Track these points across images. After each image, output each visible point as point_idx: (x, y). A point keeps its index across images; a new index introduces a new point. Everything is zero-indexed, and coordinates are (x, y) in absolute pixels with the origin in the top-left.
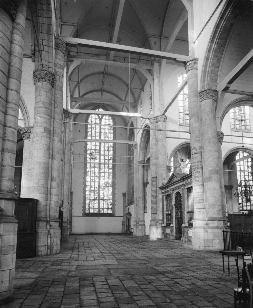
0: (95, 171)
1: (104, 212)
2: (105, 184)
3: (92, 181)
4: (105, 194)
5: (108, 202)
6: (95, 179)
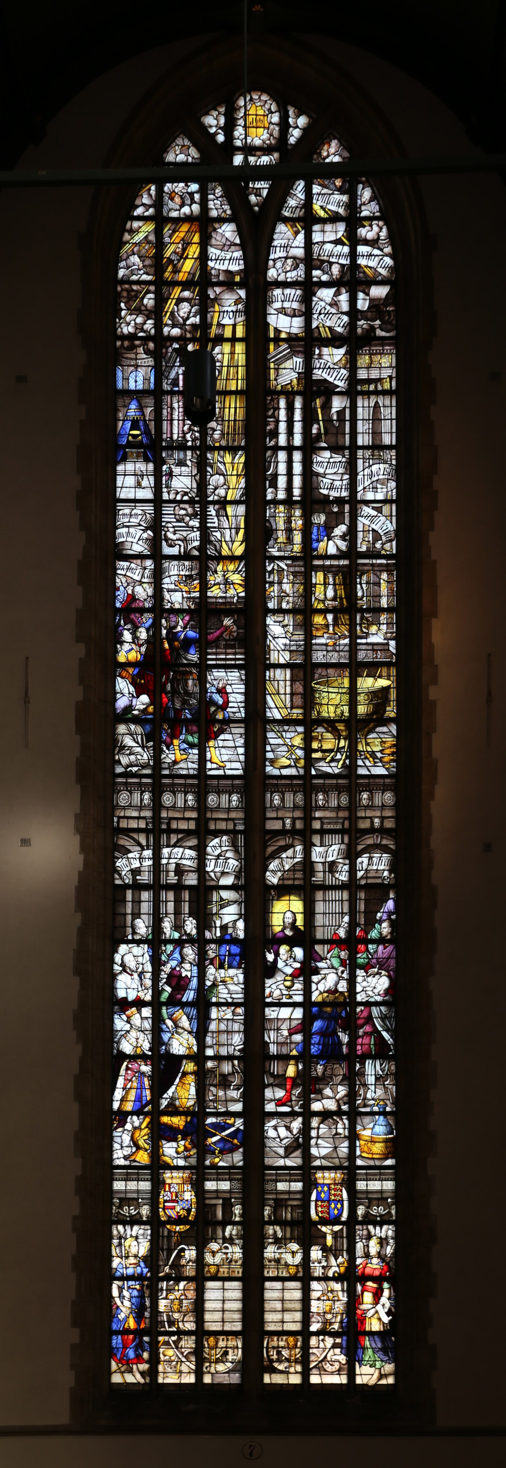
0: (201, 869)
1: (305, 1374)
2: (317, 1025)
3: (174, 1001)
4: (321, 1149)
5: (351, 1251)
6: (211, 970)
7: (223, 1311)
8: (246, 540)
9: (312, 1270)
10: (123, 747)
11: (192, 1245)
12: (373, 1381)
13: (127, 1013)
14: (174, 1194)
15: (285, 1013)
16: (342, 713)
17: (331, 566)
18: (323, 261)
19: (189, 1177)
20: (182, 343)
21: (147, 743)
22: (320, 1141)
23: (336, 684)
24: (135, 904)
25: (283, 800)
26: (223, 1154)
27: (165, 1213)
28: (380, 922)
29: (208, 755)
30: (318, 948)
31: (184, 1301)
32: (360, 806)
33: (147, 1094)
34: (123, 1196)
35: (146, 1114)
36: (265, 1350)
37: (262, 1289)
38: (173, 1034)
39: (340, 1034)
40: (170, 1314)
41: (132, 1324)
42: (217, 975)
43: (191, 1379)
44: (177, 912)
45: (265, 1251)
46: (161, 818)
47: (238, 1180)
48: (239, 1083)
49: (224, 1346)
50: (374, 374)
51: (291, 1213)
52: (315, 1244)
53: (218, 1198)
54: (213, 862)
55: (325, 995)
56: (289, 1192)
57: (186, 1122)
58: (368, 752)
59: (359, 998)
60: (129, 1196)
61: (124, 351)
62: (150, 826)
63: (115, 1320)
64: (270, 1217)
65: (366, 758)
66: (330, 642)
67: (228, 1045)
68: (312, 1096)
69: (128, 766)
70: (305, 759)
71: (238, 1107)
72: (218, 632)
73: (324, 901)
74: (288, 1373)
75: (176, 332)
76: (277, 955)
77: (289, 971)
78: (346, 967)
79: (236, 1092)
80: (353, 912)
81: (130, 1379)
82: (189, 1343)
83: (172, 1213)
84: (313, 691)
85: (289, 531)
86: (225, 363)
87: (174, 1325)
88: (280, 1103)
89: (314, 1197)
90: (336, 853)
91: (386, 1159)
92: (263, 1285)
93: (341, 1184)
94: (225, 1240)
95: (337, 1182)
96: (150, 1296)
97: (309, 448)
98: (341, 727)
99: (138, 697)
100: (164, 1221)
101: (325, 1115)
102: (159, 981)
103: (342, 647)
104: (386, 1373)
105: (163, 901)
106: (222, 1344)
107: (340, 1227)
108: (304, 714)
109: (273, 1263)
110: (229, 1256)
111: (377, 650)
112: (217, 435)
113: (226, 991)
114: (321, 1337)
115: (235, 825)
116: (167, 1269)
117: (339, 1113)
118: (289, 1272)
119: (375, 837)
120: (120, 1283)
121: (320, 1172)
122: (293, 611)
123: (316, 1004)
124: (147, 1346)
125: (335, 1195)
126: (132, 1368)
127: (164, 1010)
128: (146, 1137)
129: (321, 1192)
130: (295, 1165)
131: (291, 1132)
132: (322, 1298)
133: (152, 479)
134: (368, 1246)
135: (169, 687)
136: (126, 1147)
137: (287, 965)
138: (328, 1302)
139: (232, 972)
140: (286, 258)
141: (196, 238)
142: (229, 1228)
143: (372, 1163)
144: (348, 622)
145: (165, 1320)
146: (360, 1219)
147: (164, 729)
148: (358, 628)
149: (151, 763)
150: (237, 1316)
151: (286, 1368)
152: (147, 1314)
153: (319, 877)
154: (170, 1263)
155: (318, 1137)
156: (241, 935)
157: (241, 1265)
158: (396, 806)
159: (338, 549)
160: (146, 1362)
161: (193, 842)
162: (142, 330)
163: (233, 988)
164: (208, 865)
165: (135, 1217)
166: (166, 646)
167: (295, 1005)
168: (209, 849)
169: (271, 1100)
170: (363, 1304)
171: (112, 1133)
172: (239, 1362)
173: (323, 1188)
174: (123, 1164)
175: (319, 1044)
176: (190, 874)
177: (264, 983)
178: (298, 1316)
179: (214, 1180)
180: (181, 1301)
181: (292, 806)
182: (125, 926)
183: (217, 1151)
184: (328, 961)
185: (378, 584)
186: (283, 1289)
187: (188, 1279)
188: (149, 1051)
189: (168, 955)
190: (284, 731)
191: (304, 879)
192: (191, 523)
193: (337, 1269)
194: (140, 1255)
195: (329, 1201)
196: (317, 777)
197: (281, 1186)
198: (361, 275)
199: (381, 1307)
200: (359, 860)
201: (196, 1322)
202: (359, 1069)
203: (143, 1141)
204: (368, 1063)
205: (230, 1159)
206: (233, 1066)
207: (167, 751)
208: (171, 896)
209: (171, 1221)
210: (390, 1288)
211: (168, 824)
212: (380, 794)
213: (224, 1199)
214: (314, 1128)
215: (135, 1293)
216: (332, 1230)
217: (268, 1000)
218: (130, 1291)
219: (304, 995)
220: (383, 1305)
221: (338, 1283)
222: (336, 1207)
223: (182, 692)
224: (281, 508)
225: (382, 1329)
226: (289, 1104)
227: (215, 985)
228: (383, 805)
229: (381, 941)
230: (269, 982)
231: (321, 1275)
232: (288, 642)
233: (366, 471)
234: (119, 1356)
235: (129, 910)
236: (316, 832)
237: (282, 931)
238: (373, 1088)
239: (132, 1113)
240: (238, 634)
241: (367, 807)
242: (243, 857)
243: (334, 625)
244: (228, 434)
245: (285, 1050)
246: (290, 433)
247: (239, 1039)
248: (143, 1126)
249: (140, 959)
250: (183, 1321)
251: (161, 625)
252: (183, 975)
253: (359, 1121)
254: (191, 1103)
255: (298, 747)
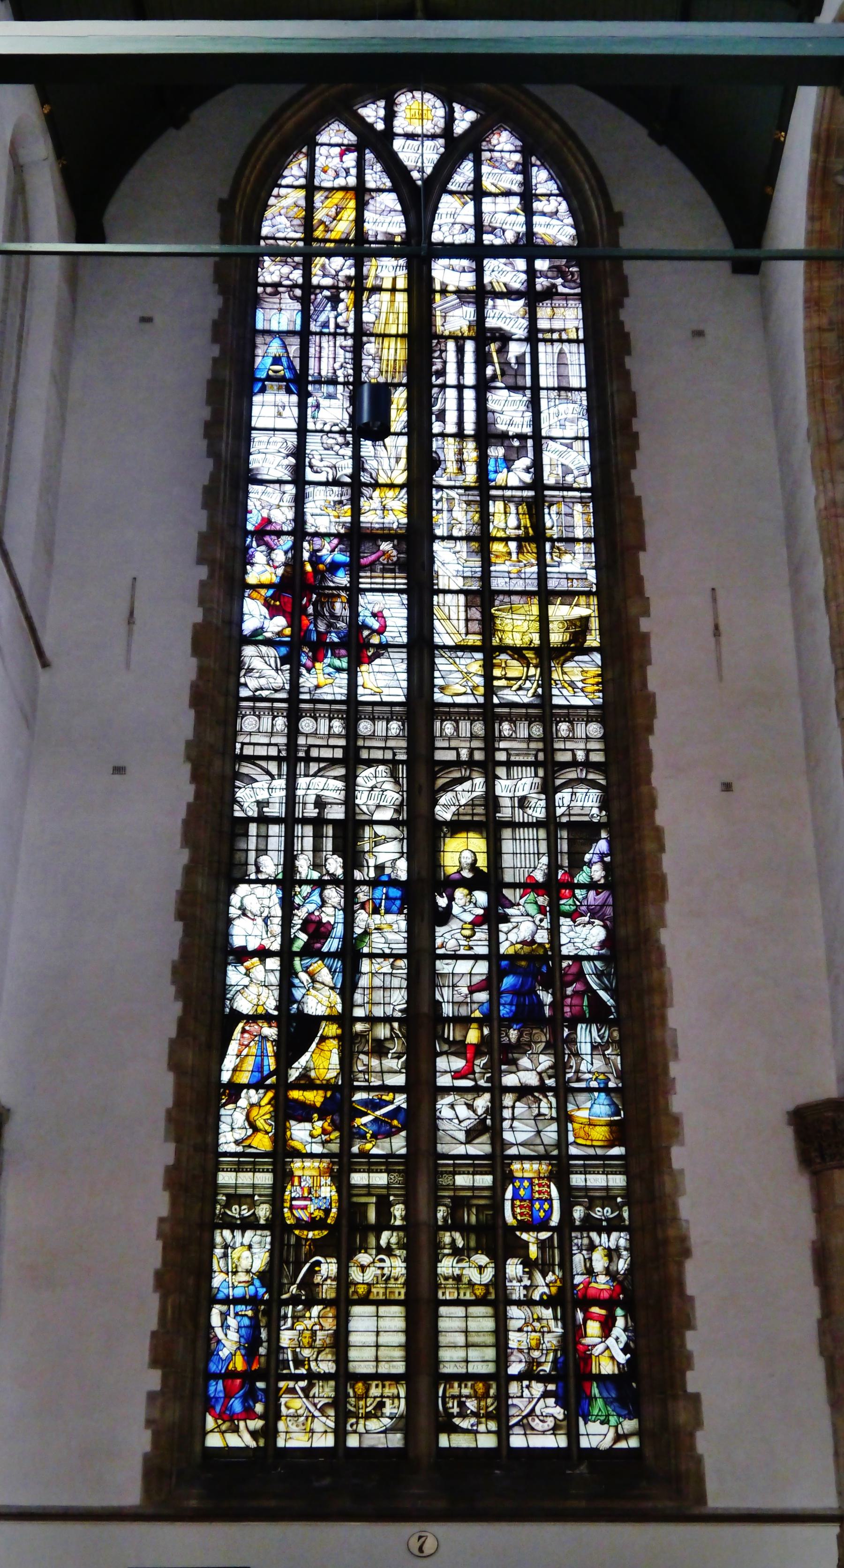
0: (349, 801)
1: (503, 1433)
2: (508, 981)
3: (309, 951)
7: (377, 1346)
8: (409, 468)
9: (508, 1291)
10: (250, 670)
11: (332, 1256)
12: (606, 1444)
13: (245, 964)
14: (306, 1190)
15: (463, 966)
16: (531, 642)
17: (512, 497)
18: (495, 228)
19: (328, 1168)
20: (334, 290)
21: (282, 665)
22: (516, 1124)
23: (522, 611)
24: (260, 839)
25: (457, 729)
26: (377, 1139)
27: (292, 1214)
28: (590, 864)
29: (360, 681)
30: (508, 893)
31: (318, 1333)
32: (557, 737)
33: (271, 1063)
34: (232, 1191)
35: (268, 1088)
36: (440, 1400)
37: (436, 1317)
38: (308, 990)
39: (540, 993)
40: (298, 1350)
41: (239, 1364)
42: (370, 921)
43: (329, 1441)
44: (317, 849)
45: (439, 1265)
46: (297, 745)
47: (399, 1171)
48: (400, 1050)
49: (379, 1395)
50: (557, 325)
51: (477, 1216)
52: (513, 1257)
53: (369, 1195)
54: (366, 794)
55: (519, 946)
56: (473, 1188)
57: (325, 1097)
58: (565, 681)
59: (565, 951)
60: (241, 1191)
61: (265, 296)
62: (284, 754)
63: (215, 1358)
64: (445, 1219)
65: (563, 687)
66: (514, 570)
67: (384, 1004)
68: (503, 1067)
69: (257, 690)
70: (485, 686)
71: (400, 1080)
72: (373, 557)
73: (514, 839)
74: (476, 1432)
75: (328, 282)
76: (451, 899)
77: (469, 918)
78: (545, 915)
79: (396, 1061)
80: (552, 852)
81: (234, 1441)
82: (325, 1391)
83: (304, 1215)
84: (493, 618)
85: (461, 462)
86: (384, 309)
87: (303, 1366)
88: (458, 1075)
89: (509, 1194)
90: (527, 787)
91: (611, 1146)
92: (437, 1311)
93: (549, 1179)
94: (379, 1250)
95: (542, 1175)
96: (268, 1326)
97: (483, 387)
98: (530, 655)
99: (271, 619)
100: (291, 1225)
101: (522, 1092)
102: (290, 927)
103: (527, 576)
104: (626, 1432)
105: (298, 837)
106: (374, 1391)
107: (549, 1234)
108: (483, 640)
109: (450, 1281)
110: (386, 1271)
111: (572, 579)
112: (372, 373)
113: (383, 940)
114: (526, 1383)
115: (394, 754)
116: (294, 1289)
117: (542, 1088)
118: (475, 1294)
119: (579, 771)
120: (224, 1308)
121: (518, 1162)
122: (468, 538)
123: (506, 957)
124: (261, 1395)
125: (540, 1192)
126: (238, 1426)
127: (297, 962)
128: (268, 1116)
129: (519, 1188)
130: (482, 1153)
131: (474, 1111)
132: (525, 1329)
133: (295, 411)
134: (590, 1259)
135: (310, 610)
136: (239, 1128)
137: (465, 911)
138: (533, 1334)
139: (390, 918)
140: (453, 224)
141: (352, 204)
142: (385, 1235)
143: (591, 1151)
144: (535, 550)
145: (290, 1358)
146: (577, 1223)
147: (304, 652)
148: (548, 557)
149: (287, 687)
150: (399, 1353)
151: (472, 1425)
152: (262, 1351)
153: (505, 813)
154: (298, 1281)
155: (513, 1119)
156: (403, 876)
157: (404, 1284)
158: (604, 738)
159: (521, 480)
160: (260, 1417)
161: (341, 771)
162: (288, 278)
163: (391, 936)
164: (359, 797)
165: (248, 1220)
166: (308, 568)
167: (477, 958)
168: (359, 780)
169: (446, 1072)
170: (586, 1336)
171: (219, 1111)
172: (401, 1417)
173: (522, 1183)
174: (233, 1150)
175: (511, 1004)
176: (335, 806)
177: (434, 932)
178: (491, 1353)
179: (364, 1171)
180: (314, 1333)
181: (469, 735)
182: (246, 864)
183: (368, 1135)
184: (521, 907)
185: (571, 515)
186: (466, 1317)
187: (326, 1303)
188: (275, 1009)
189: (304, 898)
190: (458, 657)
191: (486, 815)
192: (342, 452)
193: (546, 1290)
194: (254, 1270)
195: (532, 1200)
196: (501, 705)
197: (462, 1180)
198: (539, 241)
199: (614, 1341)
200: (558, 796)
201: (336, 1362)
202: (568, 1035)
203: (262, 1121)
204: (581, 1029)
205: (388, 1145)
206: (392, 1029)
207: (307, 675)
208: (309, 830)
209: (300, 1224)
210: (625, 1316)
211: (307, 752)
212: (584, 725)
213: (379, 1197)
214: (508, 1108)
215: (246, 1322)
216: (537, 1238)
217: (439, 951)
218: (239, 1318)
219: (489, 946)
220: (617, 1339)
221: (547, 1308)
222: (541, 1207)
223: (327, 614)
224: (451, 440)
225: (616, 1372)
226: (471, 1076)
227: (366, 933)
228: (587, 738)
229: (593, 885)
230: (440, 931)
231: (522, 1298)
232: (461, 568)
233: (552, 410)
234: (218, 1409)
235: (252, 843)
236: (501, 764)
237: (459, 872)
238: (588, 1058)
239: (248, 1086)
240: (399, 558)
241: (566, 739)
242: (405, 789)
243: (518, 553)
244: (387, 372)
245: (464, 1011)
246: (460, 371)
247: (400, 998)
248: (263, 1103)
249: (266, 902)
250: (316, 1360)
251: (302, 548)
252: (324, 920)
253: (571, 1098)
254: (333, 1074)
255: (475, 674)
